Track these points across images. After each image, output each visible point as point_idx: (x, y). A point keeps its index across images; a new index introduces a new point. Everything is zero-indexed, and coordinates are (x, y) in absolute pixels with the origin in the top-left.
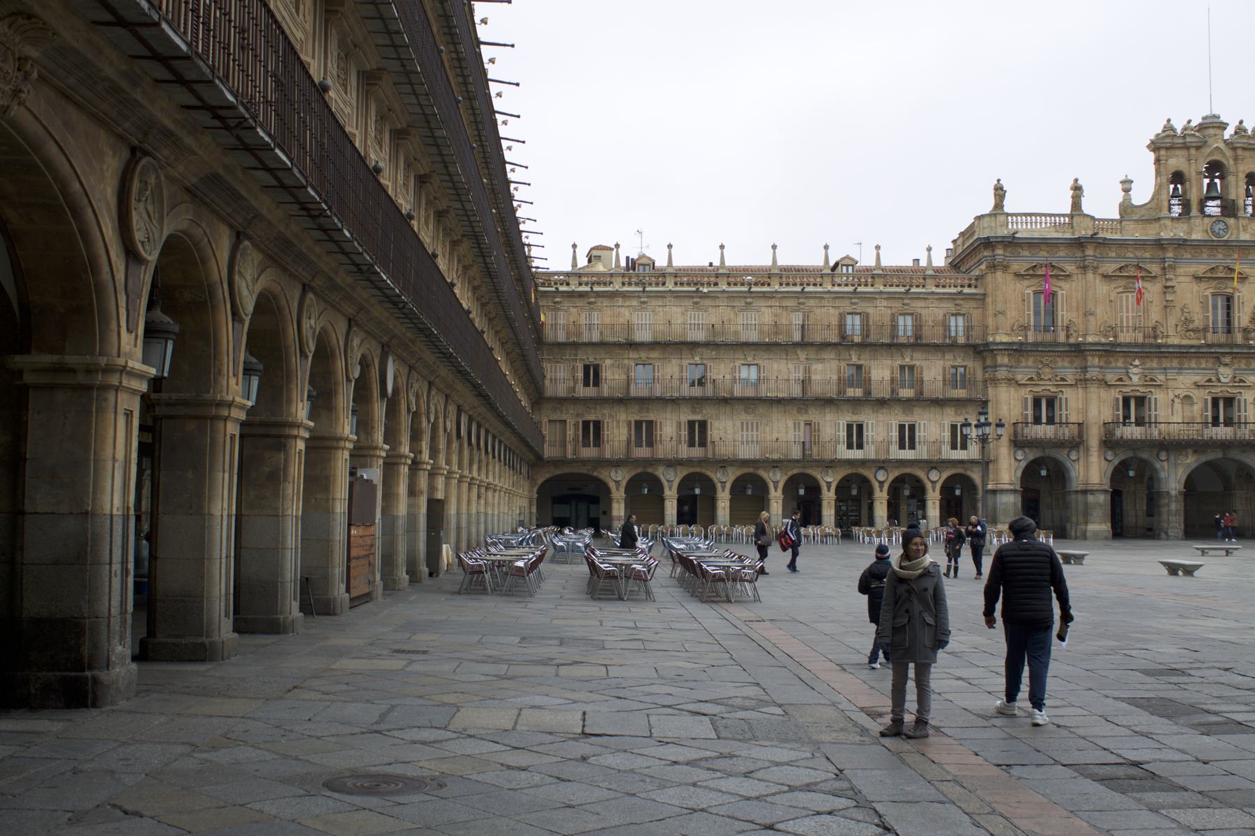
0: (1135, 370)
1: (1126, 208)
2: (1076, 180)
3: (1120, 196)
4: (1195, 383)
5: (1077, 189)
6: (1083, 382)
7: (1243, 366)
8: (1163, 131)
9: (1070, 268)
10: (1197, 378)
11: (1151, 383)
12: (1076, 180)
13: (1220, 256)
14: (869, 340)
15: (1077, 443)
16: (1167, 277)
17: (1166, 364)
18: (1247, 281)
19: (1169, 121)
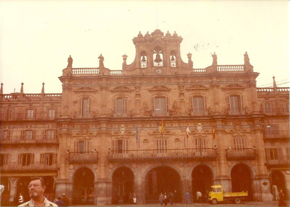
0: (122, 129)
1: (124, 65)
2: (101, 55)
3: (122, 61)
4: (149, 133)
5: (101, 58)
6: (99, 134)
7: (170, 126)
8: (138, 36)
9: (98, 88)
10: (149, 132)
11: (129, 133)
12: (101, 55)
13: (159, 82)
14: (9, 120)
15: (96, 161)
16: (137, 90)
17: (136, 125)
18: (171, 91)
19: (140, 32)
